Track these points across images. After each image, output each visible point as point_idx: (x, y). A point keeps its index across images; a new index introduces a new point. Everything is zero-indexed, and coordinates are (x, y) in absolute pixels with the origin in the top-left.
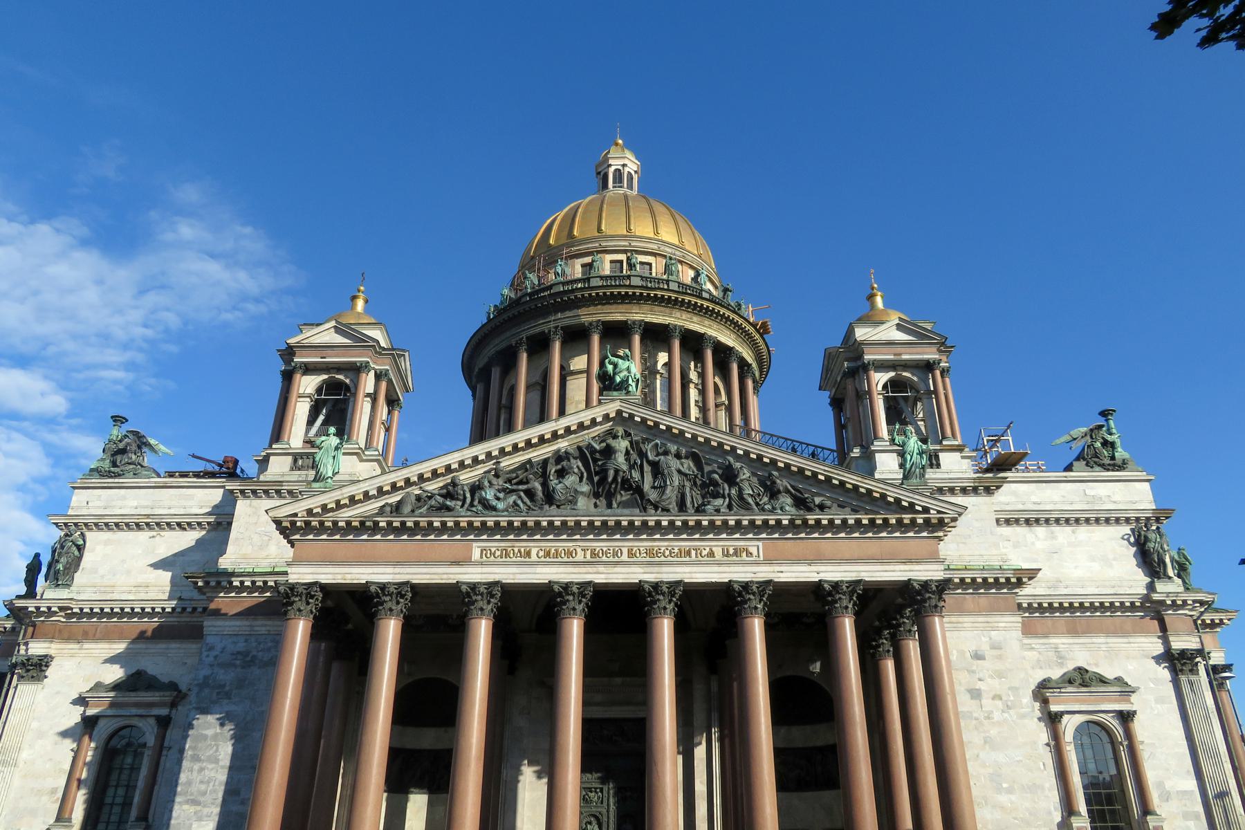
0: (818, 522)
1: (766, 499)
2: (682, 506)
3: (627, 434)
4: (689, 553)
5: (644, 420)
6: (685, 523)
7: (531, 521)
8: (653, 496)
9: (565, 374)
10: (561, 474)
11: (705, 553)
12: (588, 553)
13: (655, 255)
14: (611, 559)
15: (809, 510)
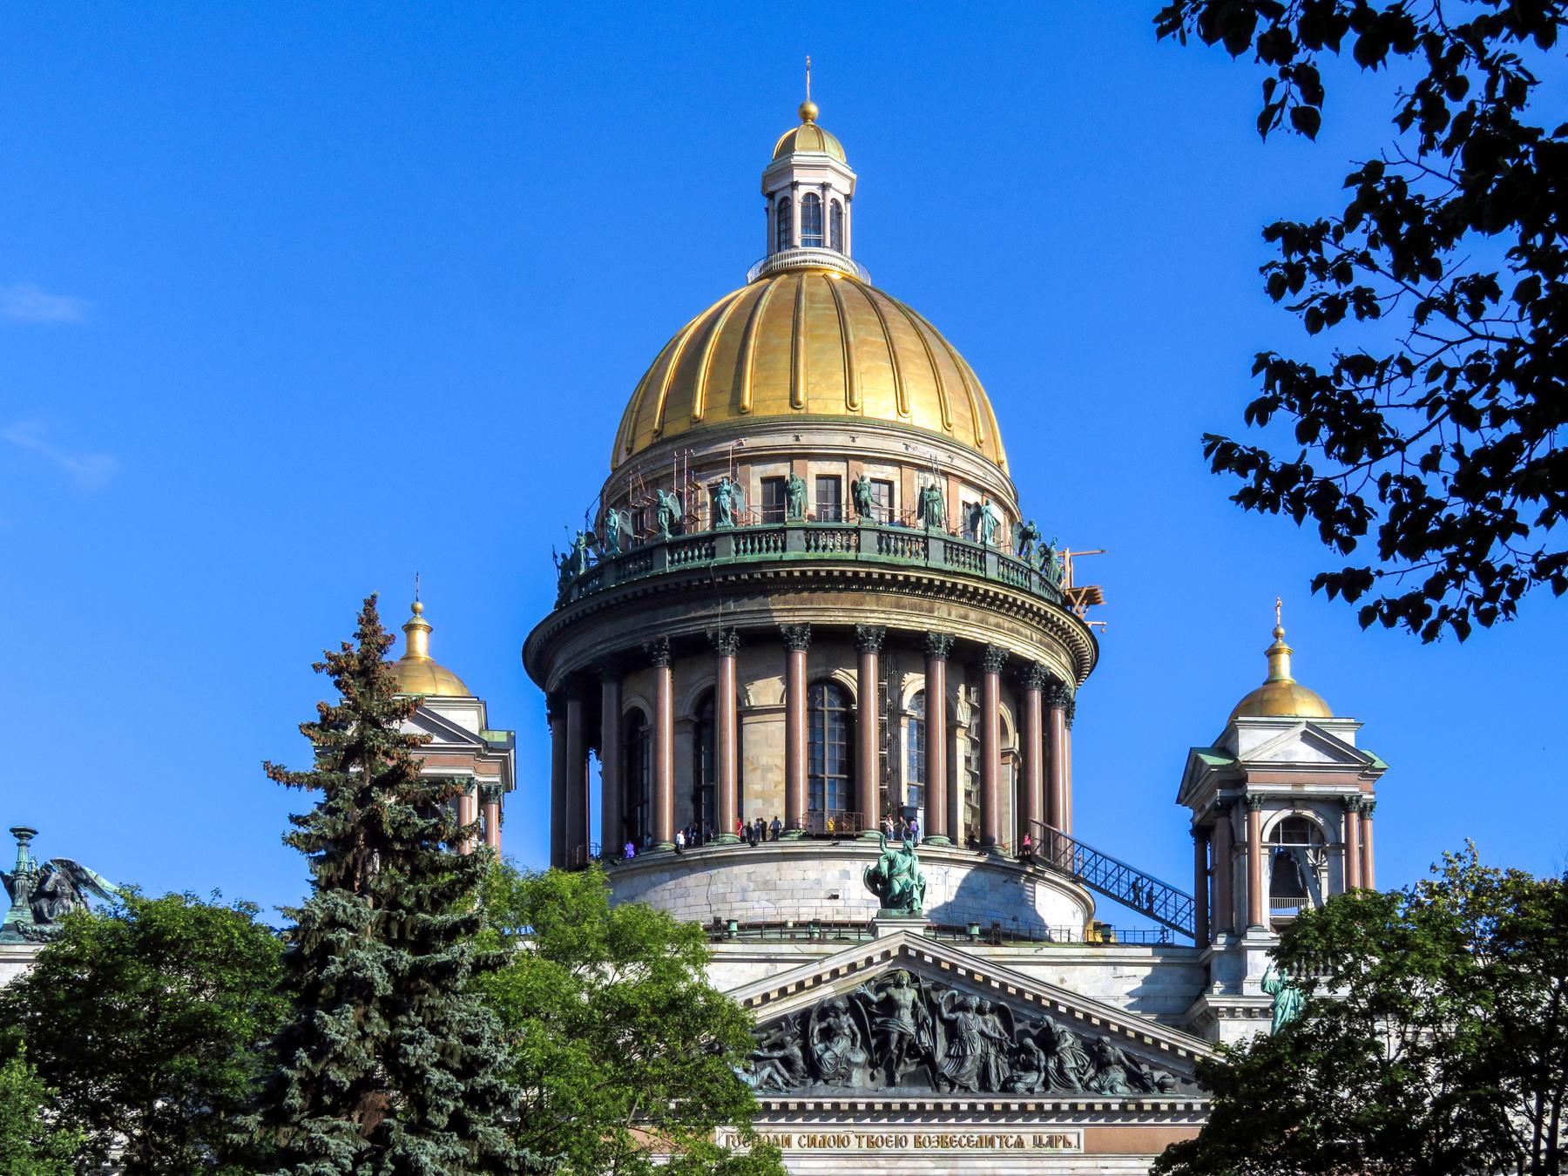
0: (1156, 1106)
1: (1091, 1072)
2: (985, 1084)
3: (914, 979)
4: (991, 1142)
5: (937, 961)
6: (989, 1107)
7: (793, 1103)
8: (948, 1068)
9: (743, 712)
10: (828, 1035)
11: (1011, 1141)
12: (864, 1140)
13: (899, 464)
14: (894, 1150)
15: (1146, 1089)
